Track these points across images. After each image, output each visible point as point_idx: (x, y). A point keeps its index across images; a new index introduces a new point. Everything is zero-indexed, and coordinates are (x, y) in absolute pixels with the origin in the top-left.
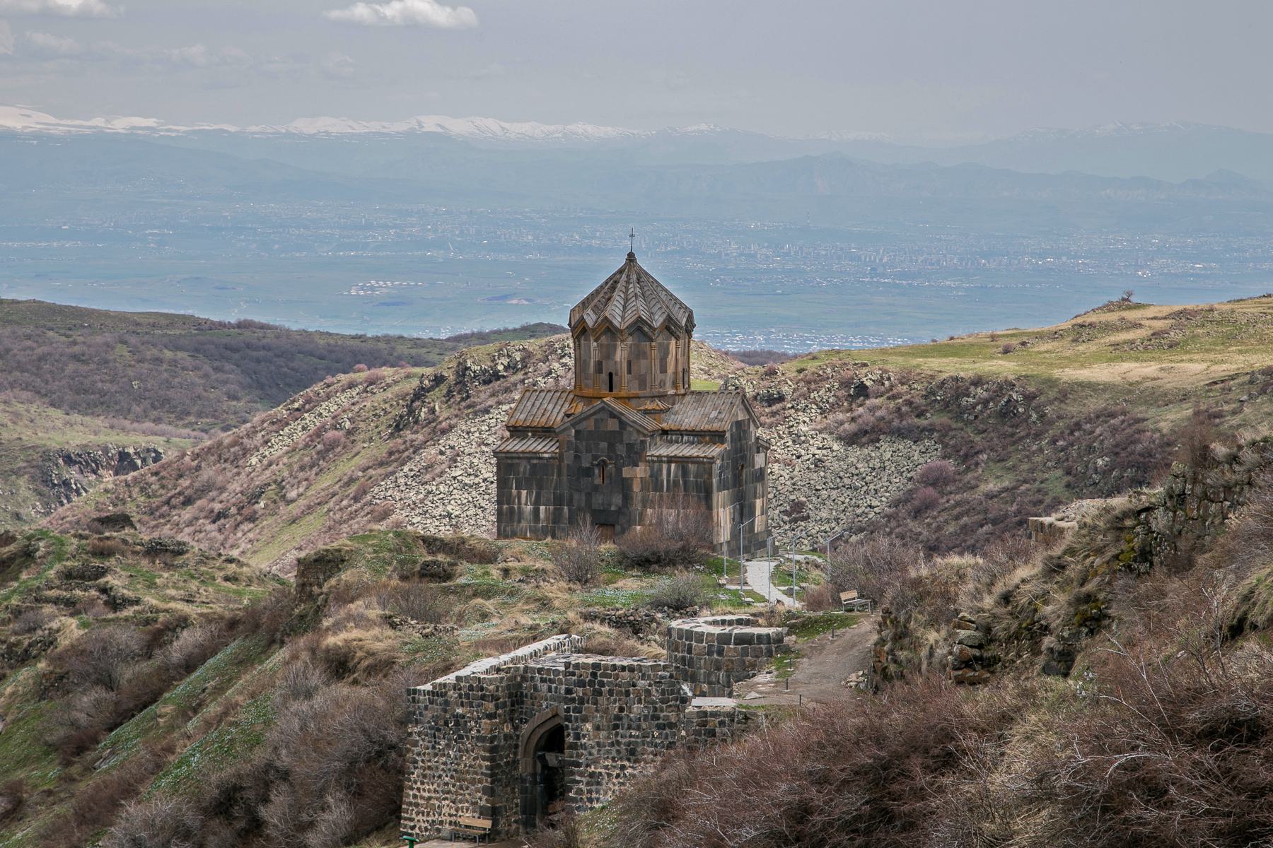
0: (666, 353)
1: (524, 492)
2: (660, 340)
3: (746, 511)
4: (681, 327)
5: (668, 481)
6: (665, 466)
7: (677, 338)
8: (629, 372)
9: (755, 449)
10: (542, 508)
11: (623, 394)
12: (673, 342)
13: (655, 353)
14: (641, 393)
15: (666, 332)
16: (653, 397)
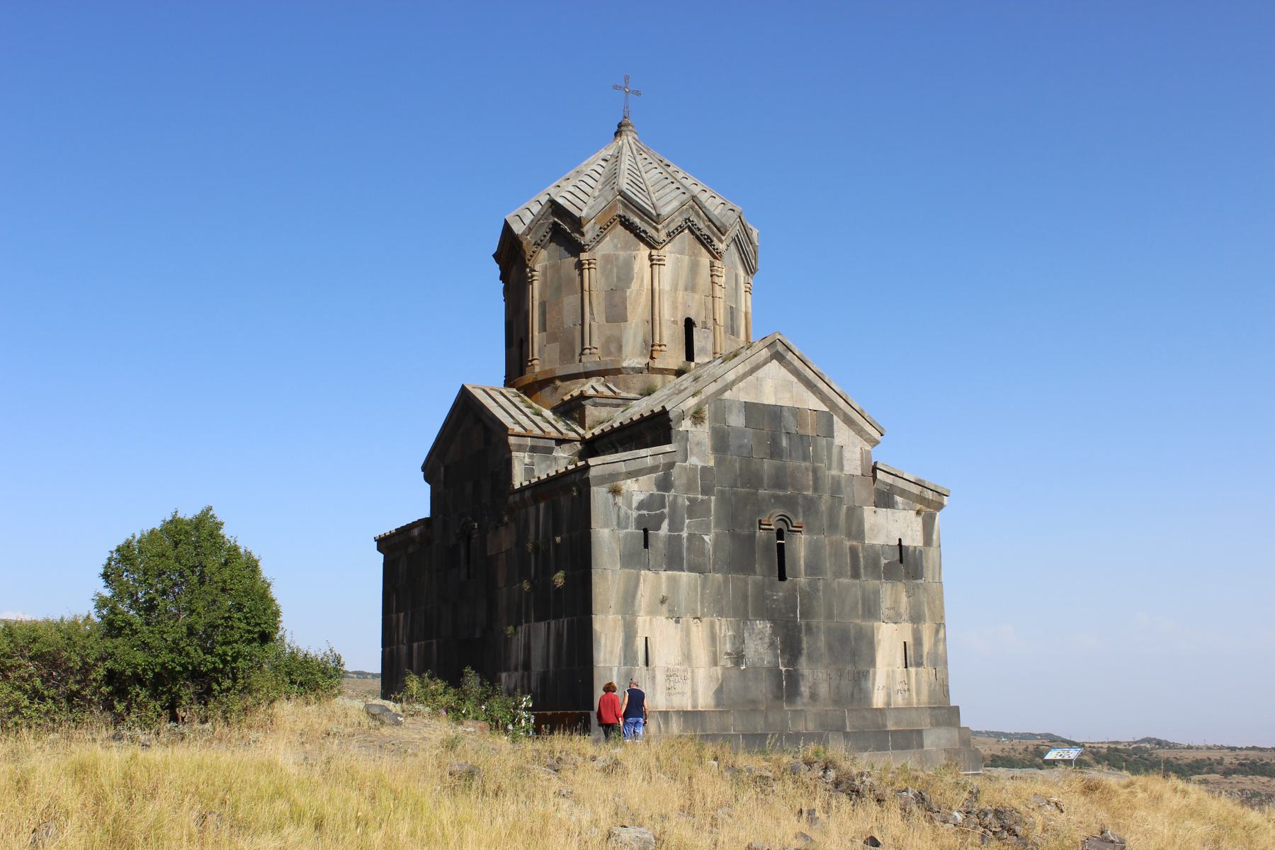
0: (626, 275)
1: (402, 615)
2: (606, 247)
3: (816, 642)
4: (655, 219)
5: (536, 548)
6: (532, 510)
7: (651, 244)
8: (543, 328)
9: (862, 492)
10: (415, 645)
11: (528, 378)
12: (644, 251)
13: (595, 278)
14: (559, 373)
15: (620, 228)
16: (588, 375)
